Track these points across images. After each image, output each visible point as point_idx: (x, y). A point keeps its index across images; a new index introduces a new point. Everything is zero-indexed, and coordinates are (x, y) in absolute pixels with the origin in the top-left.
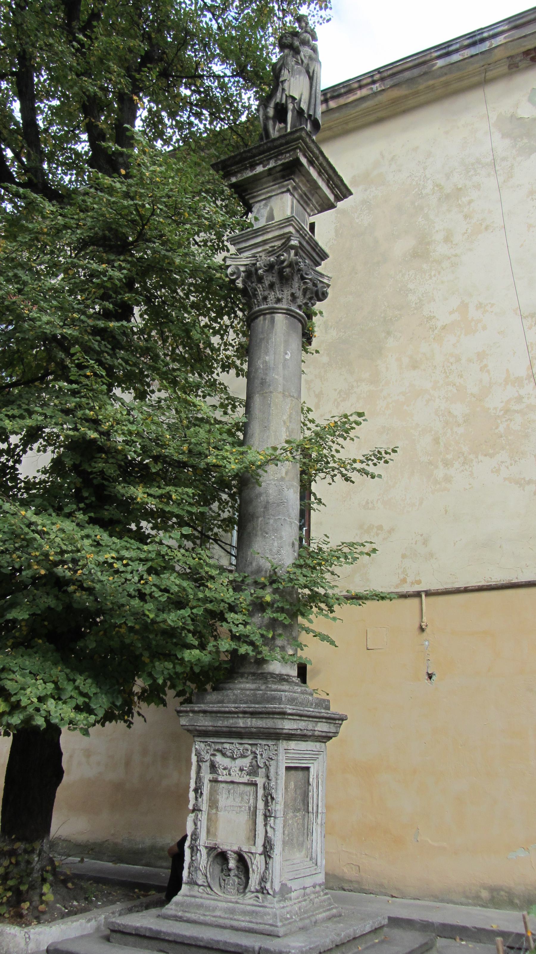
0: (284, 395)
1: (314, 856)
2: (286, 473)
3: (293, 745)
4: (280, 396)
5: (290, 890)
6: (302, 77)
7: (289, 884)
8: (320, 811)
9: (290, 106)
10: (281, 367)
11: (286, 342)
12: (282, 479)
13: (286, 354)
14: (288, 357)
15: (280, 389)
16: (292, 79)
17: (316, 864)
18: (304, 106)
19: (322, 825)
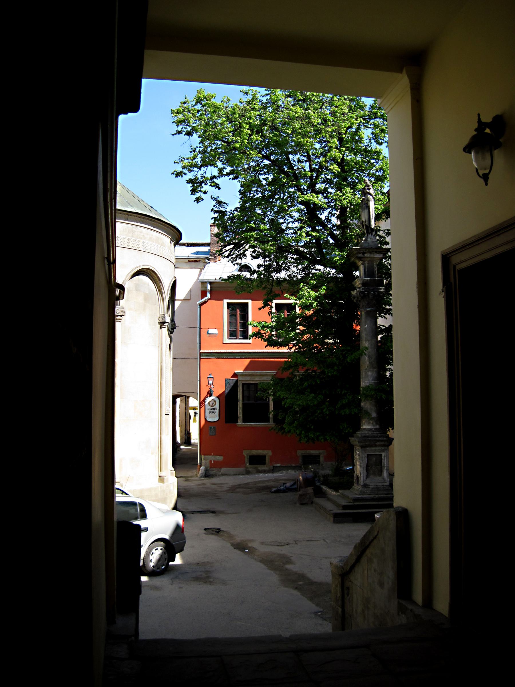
0: (366, 341)
1: (384, 478)
2: (367, 367)
3: (368, 449)
4: (364, 341)
5: (369, 485)
6: (365, 211)
7: (369, 484)
8: (386, 466)
9: (364, 224)
10: (364, 331)
11: (366, 322)
12: (366, 369)
13: (366, 326)
14: (366, 327)
15: (364, 339)
16: (362, 213)
17: (385, 480)
18: (367, 223)
19: (387, 470)
